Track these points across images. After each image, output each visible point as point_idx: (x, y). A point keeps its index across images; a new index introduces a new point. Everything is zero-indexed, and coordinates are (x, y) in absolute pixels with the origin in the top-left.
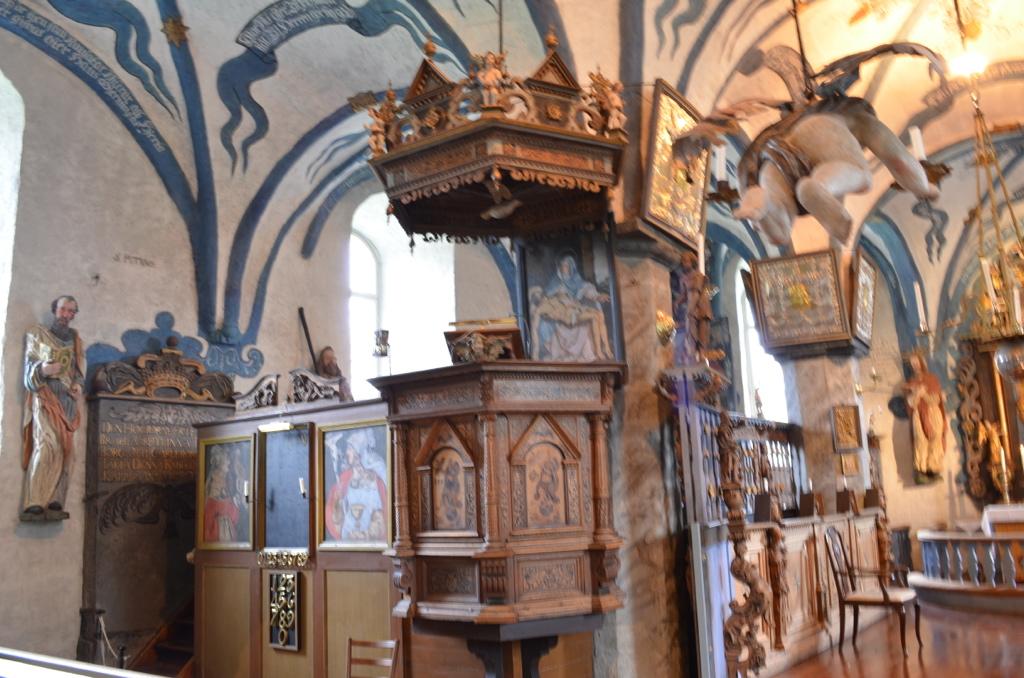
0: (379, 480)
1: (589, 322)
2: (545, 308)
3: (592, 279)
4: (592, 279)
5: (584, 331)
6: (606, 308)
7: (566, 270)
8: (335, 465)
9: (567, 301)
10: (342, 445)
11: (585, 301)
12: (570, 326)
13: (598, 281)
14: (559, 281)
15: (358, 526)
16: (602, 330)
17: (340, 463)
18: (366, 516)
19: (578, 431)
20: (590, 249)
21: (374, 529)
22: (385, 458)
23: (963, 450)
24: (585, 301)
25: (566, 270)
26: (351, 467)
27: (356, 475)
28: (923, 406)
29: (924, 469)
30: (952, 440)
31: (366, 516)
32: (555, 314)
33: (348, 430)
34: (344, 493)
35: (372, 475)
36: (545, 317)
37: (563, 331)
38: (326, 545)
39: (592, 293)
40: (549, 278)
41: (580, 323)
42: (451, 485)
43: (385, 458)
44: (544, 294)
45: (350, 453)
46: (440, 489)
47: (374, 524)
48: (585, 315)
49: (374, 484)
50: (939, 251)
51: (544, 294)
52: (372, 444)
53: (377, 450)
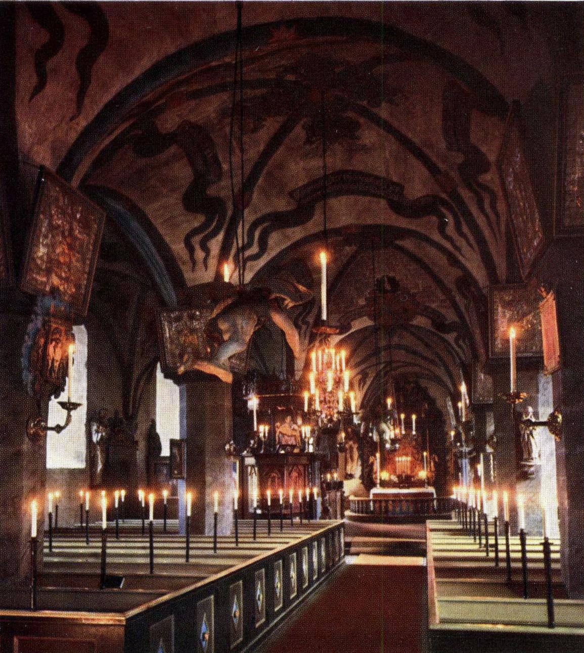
2: (281, 429)
3: (296, 423)
7: (288, 420)
12: (289, 436)
19: (301, 468)
23: (362, 465)
24: (294, 429)
25: (288, 420)
28: (351, 448)
29: (349, 473)
30: (360, 463)
36: (280, 432)
40: (283, 421)
41: (292, 436)
50: (363, 387)
51: (281, 425)
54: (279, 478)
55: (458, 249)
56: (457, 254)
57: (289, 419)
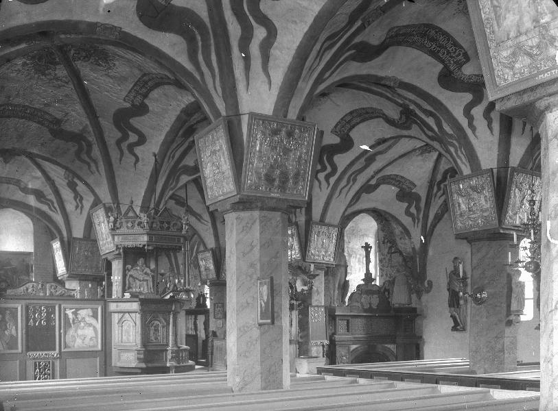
0: (94, 327)
1: (147, 280)
3: (149, 267)
4: (149, 267)
5: (145, 283)
6: (153, 277)
7: (140, 262)
8: (71, 321)
9: (140, 273)
10: (75, 314)
11: (146, 273)
13: (151, 268)
14: (138, 265)
15: (83, 343)
16: (151, 284)
17: (74, 320)
18: (87, 340)
20: (150, 258)
21: (91, 343)
22: (97, 320)
24: (146, 273)
25: (140, 262)
26: (80, 322)
27: (82, 324)
31: (87, 340)
32: (135, 276)
33: (78, 309)
34: (76, 331)
35: (90, 325)
36: (131, 276)
37: (137, 281)
38: (66, 350)
39: (149, 272)
40: (134, 264)
41: (143, 280)
42: (156, 330)
43: (97, 319)
44: (132, 268)
45: (79, 317)
46: (152, 332)
47: (92, 342)
48: (146, 278)
49: (91, 328)
51: (132, 268)
52: (91, 314)
53: (95, 316)
54: (163, 327)
55: (471, 125)
56: (469, 132)
57: (141, 261)
